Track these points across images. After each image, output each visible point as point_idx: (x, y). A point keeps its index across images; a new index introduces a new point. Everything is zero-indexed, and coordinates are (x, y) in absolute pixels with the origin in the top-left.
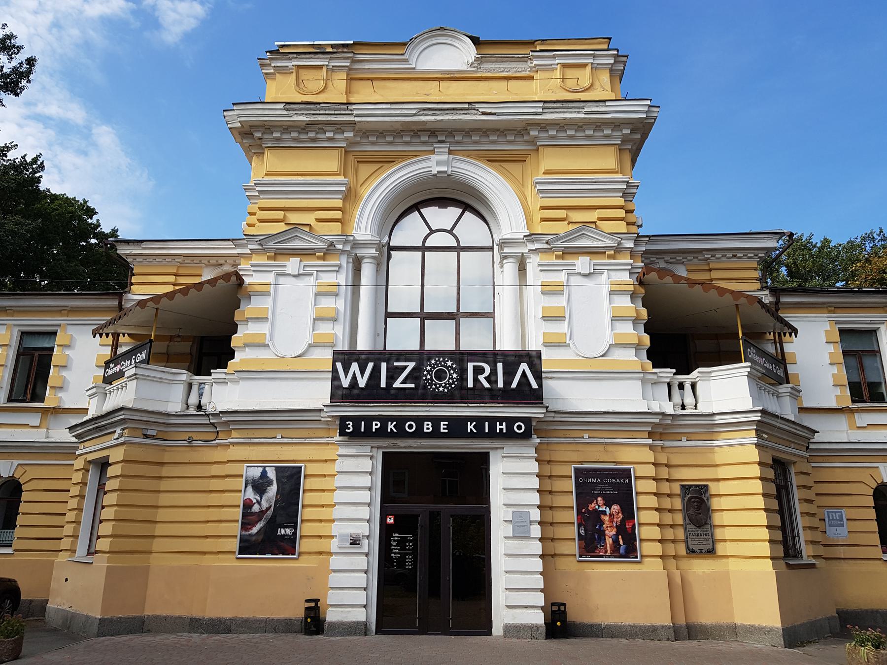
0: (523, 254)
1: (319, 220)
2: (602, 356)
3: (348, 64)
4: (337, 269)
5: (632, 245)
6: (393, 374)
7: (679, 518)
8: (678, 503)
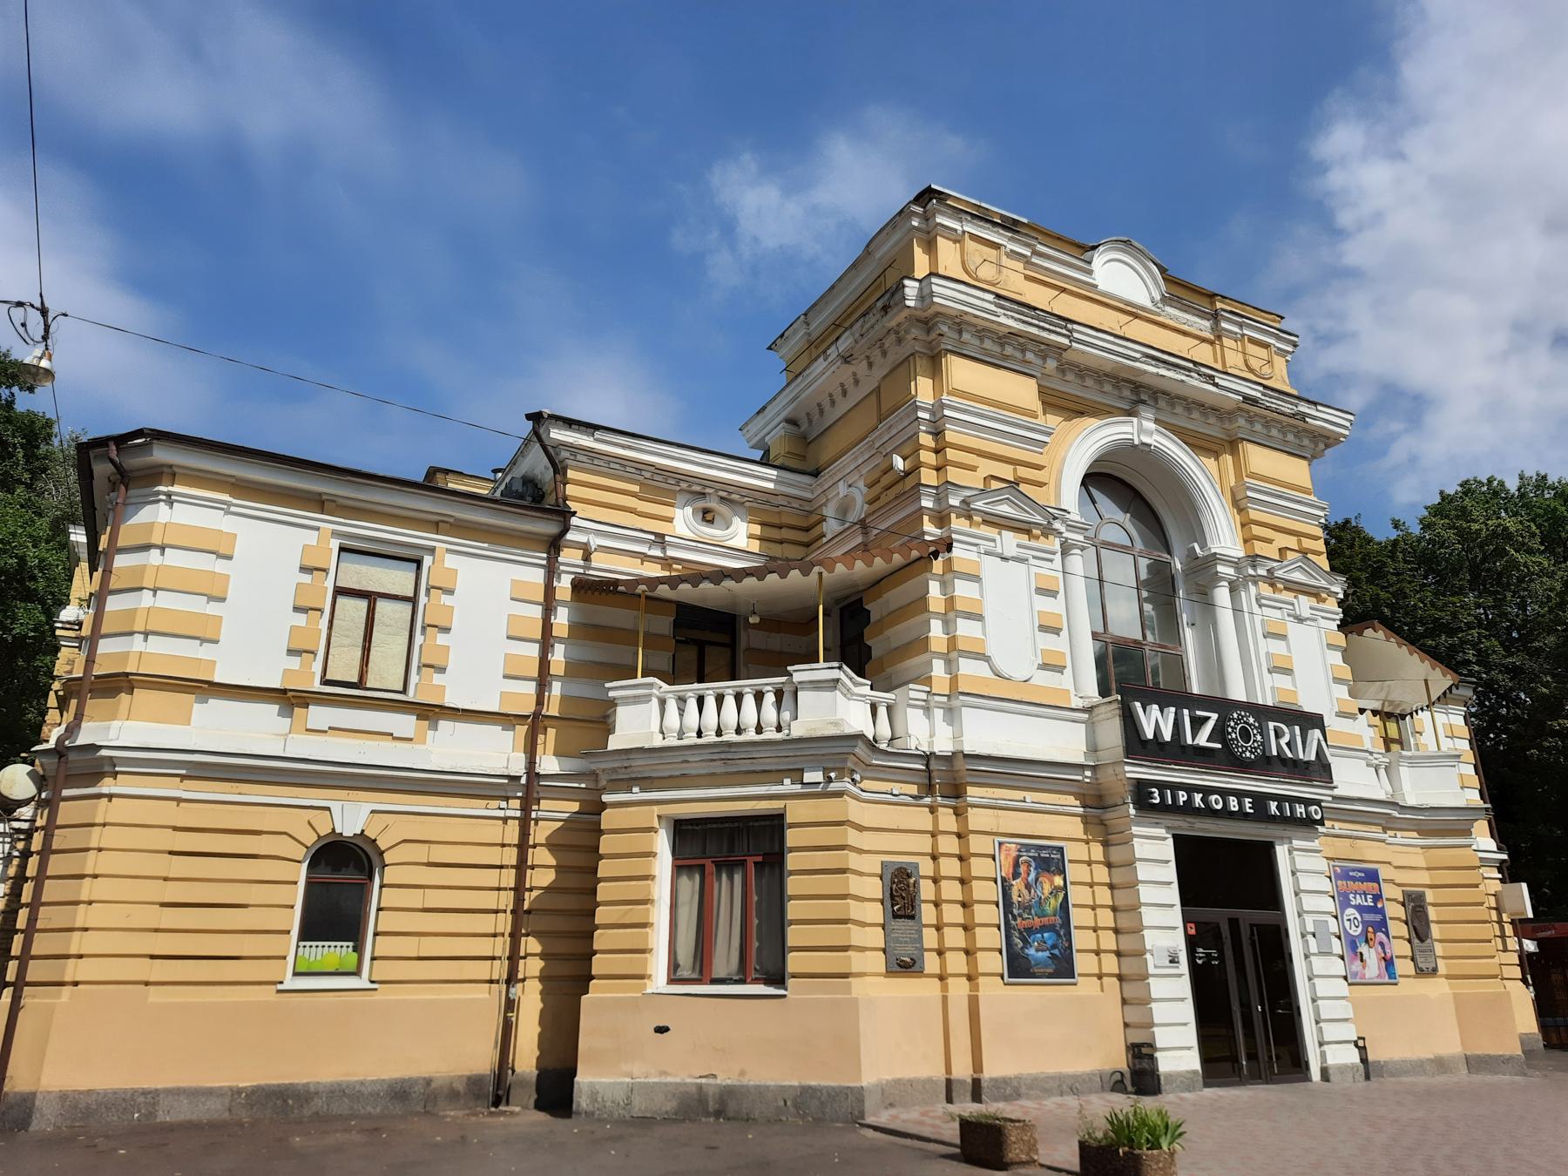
6: (1198, 723)
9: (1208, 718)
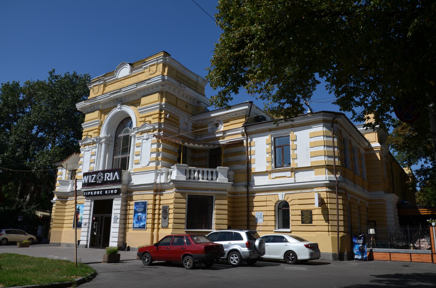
2: (148, 165)
4: (95, 147)
8: (161, 212)
9: (94, 176)
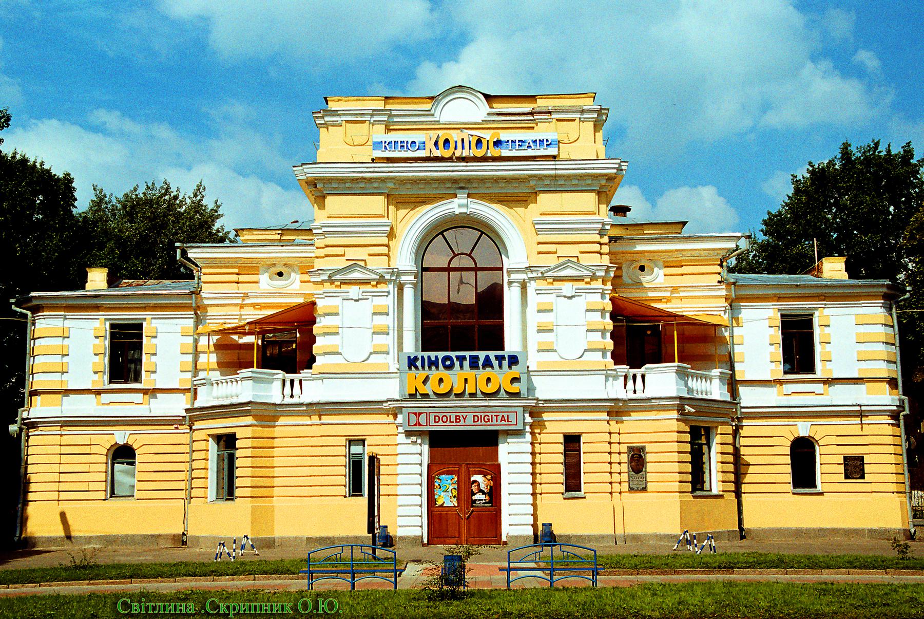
0: (524, 280)
1: (370, 255)
3: (386, 119)
4: (386, 294)
5: (603, 274)
7: (625, 467)
8: (624, 458)
